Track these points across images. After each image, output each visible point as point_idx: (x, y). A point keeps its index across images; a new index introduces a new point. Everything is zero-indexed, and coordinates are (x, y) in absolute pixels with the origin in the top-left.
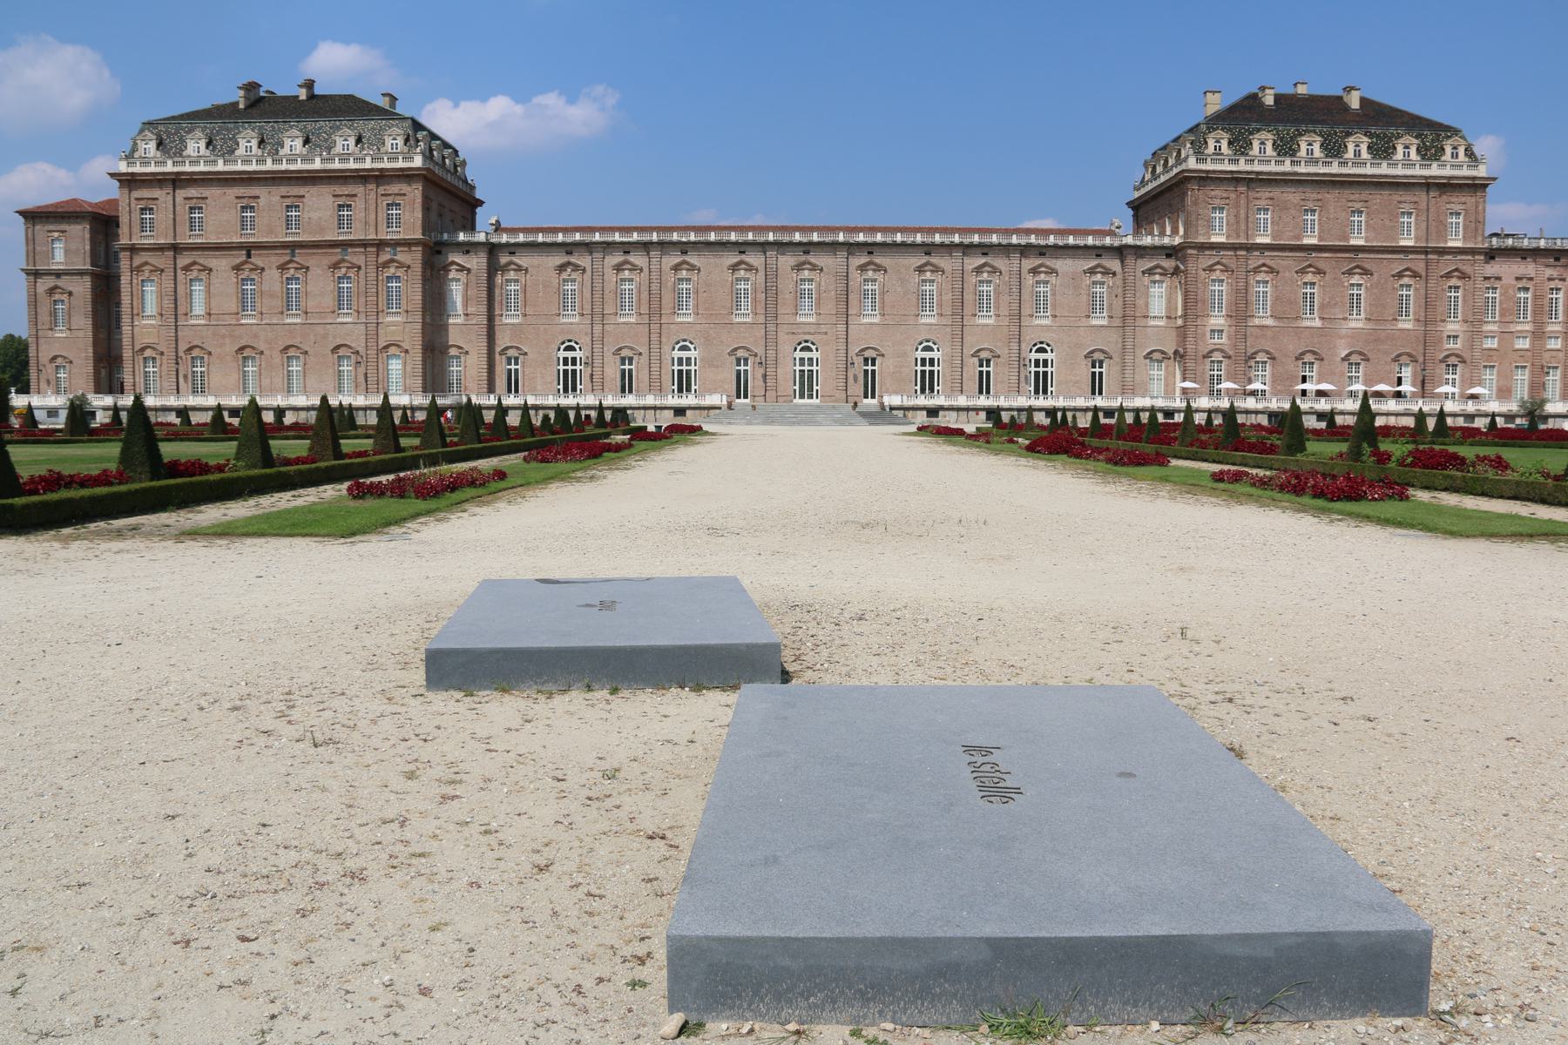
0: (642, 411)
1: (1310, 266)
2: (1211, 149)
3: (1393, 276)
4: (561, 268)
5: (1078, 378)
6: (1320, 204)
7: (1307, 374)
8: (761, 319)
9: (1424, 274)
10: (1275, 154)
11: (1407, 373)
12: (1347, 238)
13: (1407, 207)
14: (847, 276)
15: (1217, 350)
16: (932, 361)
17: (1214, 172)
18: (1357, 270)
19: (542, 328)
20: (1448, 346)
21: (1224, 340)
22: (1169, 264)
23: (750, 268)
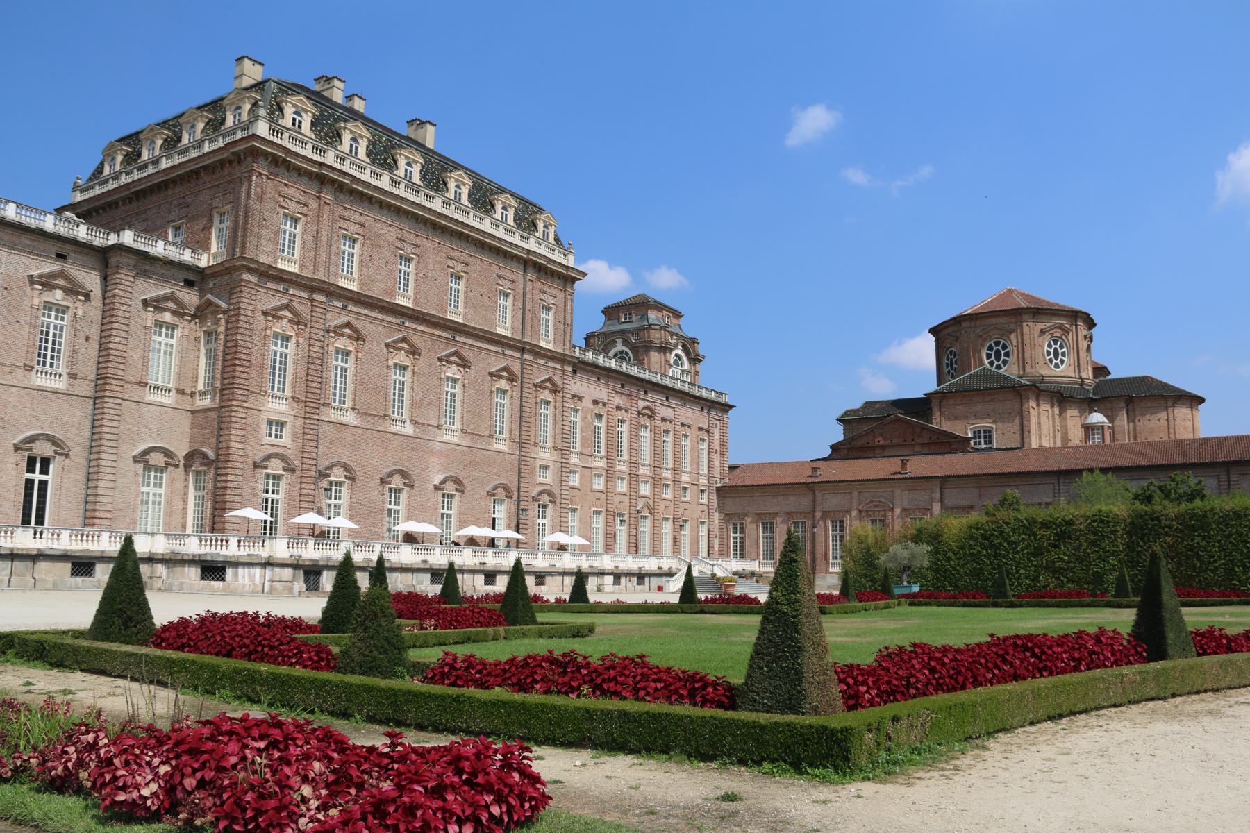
2: (287, 121)
3: (491, 375)
6: (417, 251)
11: (502, 512)
13: (506, 286)
15: (276, 455)
20: (541, 480)
21: (286, 439)
22: (191, 298)
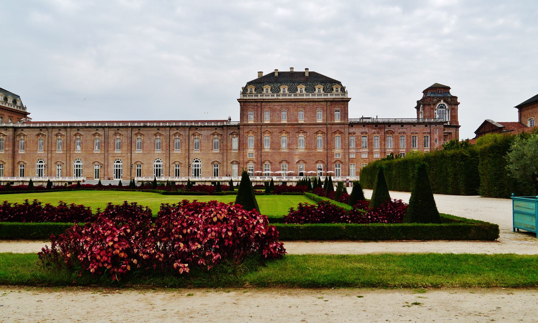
0: (58, 183)
1: (284, 130)
4: (38, 135)
5: (209, 171)
7: (284, 168)
8: (103, 152)
9: (326, 132)
10: (271, 92)
12: (297, 121)
13: (319, 109)
14: (131, 137)
15: (251, 160)
16: (198, 166)
17: (249, 99)
18: (301, 132)
19: (32, 155)
20: (336, 158)
21: (254, 157)
23: (99, 135)
